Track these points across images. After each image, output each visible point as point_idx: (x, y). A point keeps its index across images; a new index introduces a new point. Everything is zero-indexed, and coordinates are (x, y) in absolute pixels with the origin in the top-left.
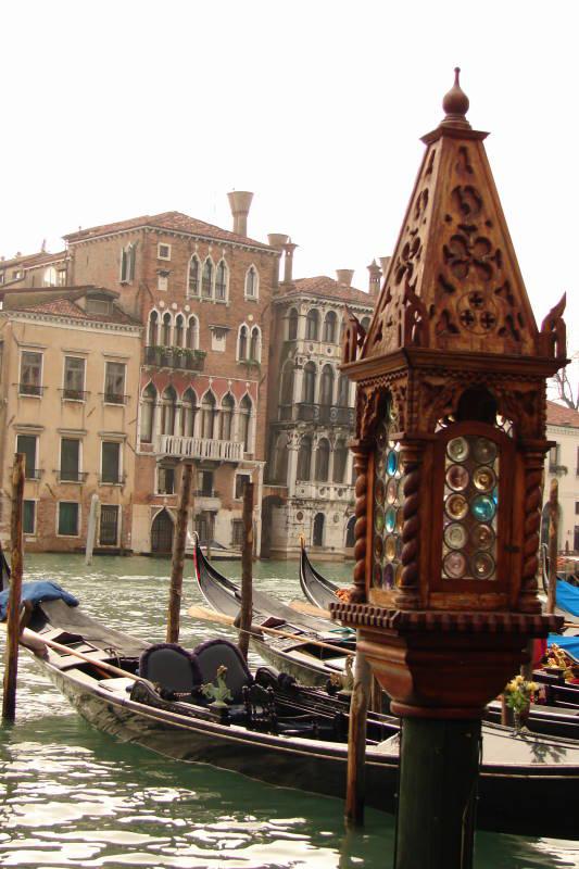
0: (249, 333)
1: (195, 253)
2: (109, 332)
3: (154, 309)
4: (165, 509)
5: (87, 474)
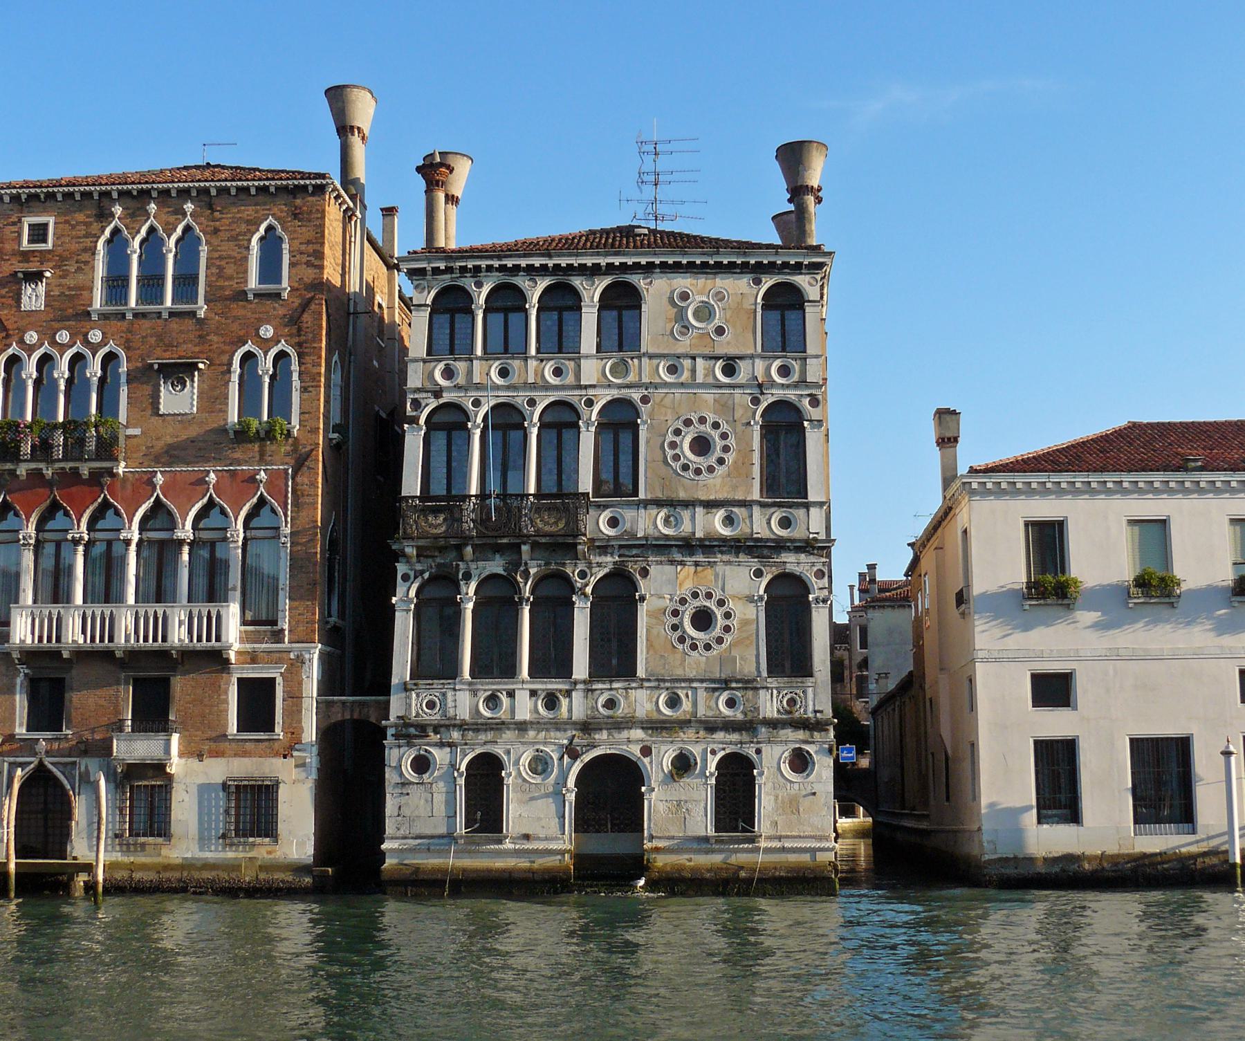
0: (266, 364)
4: (41, 763)
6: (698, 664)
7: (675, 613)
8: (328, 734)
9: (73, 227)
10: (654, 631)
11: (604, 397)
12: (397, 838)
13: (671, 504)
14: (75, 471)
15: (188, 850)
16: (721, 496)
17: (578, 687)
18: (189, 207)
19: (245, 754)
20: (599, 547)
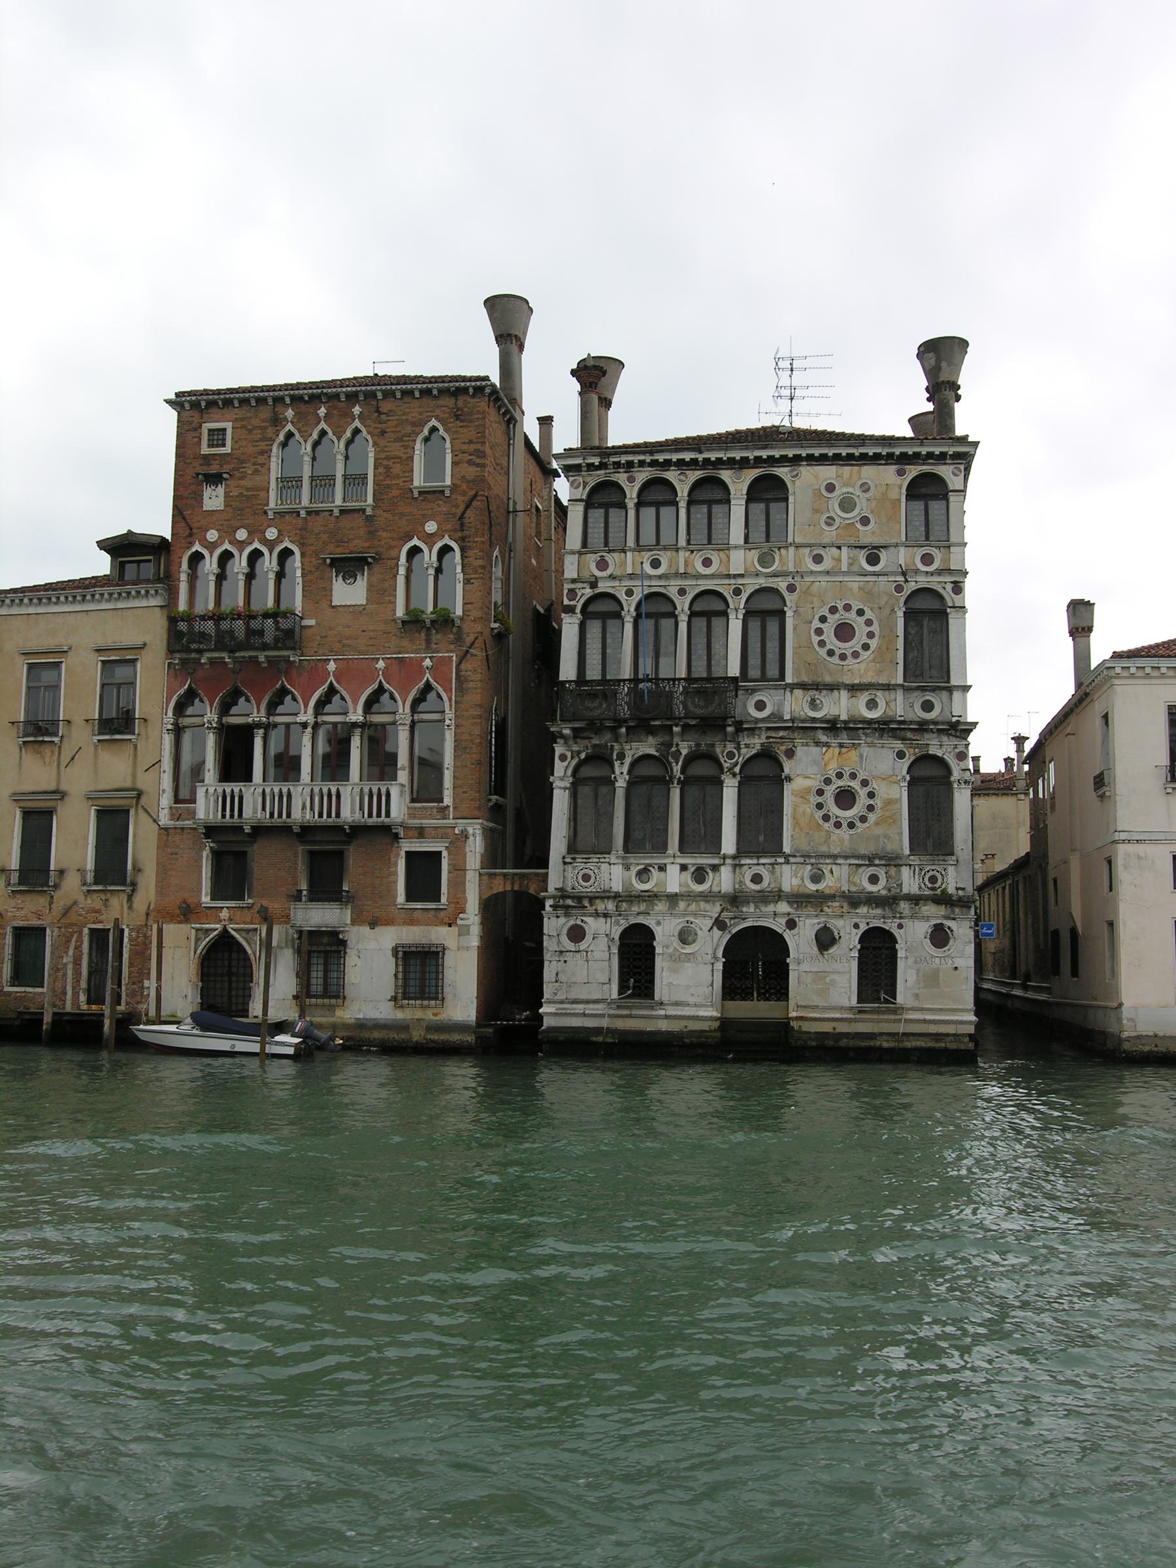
0: (429, 557)
1: (289, 427)
2: (104, 606)
3: (197, 547)
4: (225, 930)
5: (61, 872)
6: (842, 840)
7: (820, 792)
8: (489, 906)
9: (250, 431)
10: (801, 810)
11: (751, 585)
12: (554, 1002)
13: (817, 687)
14: (254, 661)
15: (360, 1011)
16: (867, 679)
17: (728, 861)
18: (357, 410)
19: (412, 922)
20: (747, 729)
